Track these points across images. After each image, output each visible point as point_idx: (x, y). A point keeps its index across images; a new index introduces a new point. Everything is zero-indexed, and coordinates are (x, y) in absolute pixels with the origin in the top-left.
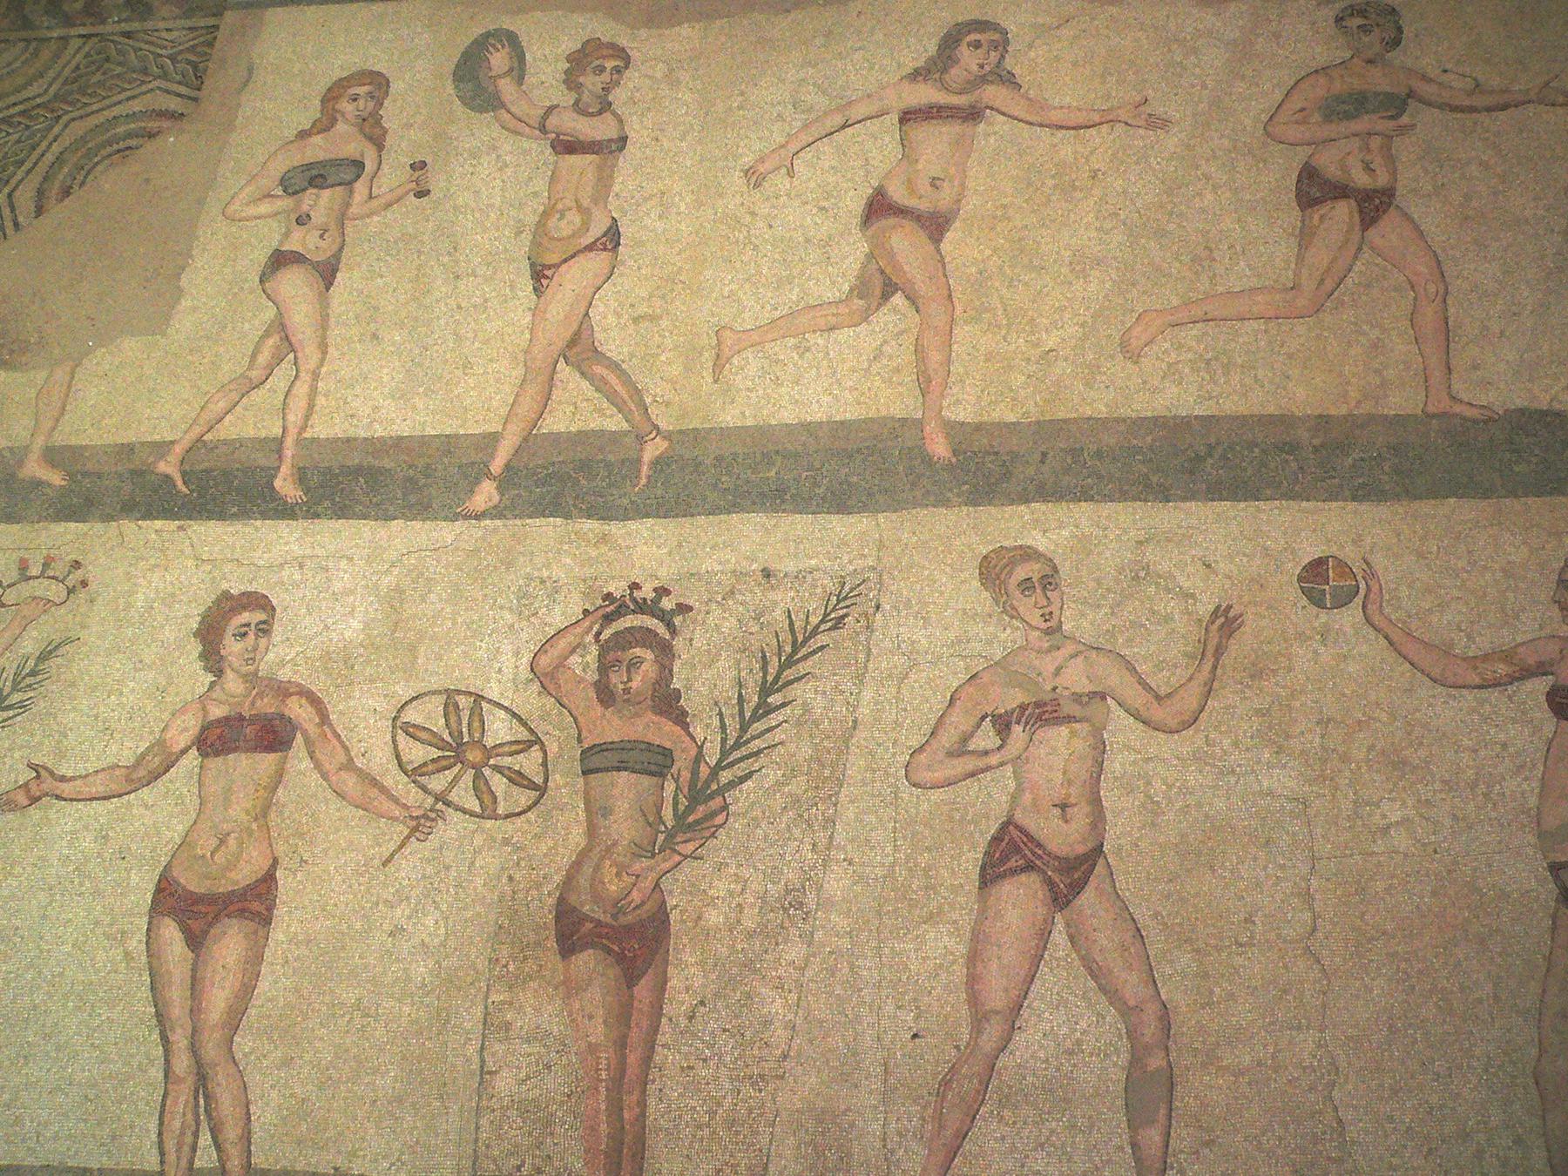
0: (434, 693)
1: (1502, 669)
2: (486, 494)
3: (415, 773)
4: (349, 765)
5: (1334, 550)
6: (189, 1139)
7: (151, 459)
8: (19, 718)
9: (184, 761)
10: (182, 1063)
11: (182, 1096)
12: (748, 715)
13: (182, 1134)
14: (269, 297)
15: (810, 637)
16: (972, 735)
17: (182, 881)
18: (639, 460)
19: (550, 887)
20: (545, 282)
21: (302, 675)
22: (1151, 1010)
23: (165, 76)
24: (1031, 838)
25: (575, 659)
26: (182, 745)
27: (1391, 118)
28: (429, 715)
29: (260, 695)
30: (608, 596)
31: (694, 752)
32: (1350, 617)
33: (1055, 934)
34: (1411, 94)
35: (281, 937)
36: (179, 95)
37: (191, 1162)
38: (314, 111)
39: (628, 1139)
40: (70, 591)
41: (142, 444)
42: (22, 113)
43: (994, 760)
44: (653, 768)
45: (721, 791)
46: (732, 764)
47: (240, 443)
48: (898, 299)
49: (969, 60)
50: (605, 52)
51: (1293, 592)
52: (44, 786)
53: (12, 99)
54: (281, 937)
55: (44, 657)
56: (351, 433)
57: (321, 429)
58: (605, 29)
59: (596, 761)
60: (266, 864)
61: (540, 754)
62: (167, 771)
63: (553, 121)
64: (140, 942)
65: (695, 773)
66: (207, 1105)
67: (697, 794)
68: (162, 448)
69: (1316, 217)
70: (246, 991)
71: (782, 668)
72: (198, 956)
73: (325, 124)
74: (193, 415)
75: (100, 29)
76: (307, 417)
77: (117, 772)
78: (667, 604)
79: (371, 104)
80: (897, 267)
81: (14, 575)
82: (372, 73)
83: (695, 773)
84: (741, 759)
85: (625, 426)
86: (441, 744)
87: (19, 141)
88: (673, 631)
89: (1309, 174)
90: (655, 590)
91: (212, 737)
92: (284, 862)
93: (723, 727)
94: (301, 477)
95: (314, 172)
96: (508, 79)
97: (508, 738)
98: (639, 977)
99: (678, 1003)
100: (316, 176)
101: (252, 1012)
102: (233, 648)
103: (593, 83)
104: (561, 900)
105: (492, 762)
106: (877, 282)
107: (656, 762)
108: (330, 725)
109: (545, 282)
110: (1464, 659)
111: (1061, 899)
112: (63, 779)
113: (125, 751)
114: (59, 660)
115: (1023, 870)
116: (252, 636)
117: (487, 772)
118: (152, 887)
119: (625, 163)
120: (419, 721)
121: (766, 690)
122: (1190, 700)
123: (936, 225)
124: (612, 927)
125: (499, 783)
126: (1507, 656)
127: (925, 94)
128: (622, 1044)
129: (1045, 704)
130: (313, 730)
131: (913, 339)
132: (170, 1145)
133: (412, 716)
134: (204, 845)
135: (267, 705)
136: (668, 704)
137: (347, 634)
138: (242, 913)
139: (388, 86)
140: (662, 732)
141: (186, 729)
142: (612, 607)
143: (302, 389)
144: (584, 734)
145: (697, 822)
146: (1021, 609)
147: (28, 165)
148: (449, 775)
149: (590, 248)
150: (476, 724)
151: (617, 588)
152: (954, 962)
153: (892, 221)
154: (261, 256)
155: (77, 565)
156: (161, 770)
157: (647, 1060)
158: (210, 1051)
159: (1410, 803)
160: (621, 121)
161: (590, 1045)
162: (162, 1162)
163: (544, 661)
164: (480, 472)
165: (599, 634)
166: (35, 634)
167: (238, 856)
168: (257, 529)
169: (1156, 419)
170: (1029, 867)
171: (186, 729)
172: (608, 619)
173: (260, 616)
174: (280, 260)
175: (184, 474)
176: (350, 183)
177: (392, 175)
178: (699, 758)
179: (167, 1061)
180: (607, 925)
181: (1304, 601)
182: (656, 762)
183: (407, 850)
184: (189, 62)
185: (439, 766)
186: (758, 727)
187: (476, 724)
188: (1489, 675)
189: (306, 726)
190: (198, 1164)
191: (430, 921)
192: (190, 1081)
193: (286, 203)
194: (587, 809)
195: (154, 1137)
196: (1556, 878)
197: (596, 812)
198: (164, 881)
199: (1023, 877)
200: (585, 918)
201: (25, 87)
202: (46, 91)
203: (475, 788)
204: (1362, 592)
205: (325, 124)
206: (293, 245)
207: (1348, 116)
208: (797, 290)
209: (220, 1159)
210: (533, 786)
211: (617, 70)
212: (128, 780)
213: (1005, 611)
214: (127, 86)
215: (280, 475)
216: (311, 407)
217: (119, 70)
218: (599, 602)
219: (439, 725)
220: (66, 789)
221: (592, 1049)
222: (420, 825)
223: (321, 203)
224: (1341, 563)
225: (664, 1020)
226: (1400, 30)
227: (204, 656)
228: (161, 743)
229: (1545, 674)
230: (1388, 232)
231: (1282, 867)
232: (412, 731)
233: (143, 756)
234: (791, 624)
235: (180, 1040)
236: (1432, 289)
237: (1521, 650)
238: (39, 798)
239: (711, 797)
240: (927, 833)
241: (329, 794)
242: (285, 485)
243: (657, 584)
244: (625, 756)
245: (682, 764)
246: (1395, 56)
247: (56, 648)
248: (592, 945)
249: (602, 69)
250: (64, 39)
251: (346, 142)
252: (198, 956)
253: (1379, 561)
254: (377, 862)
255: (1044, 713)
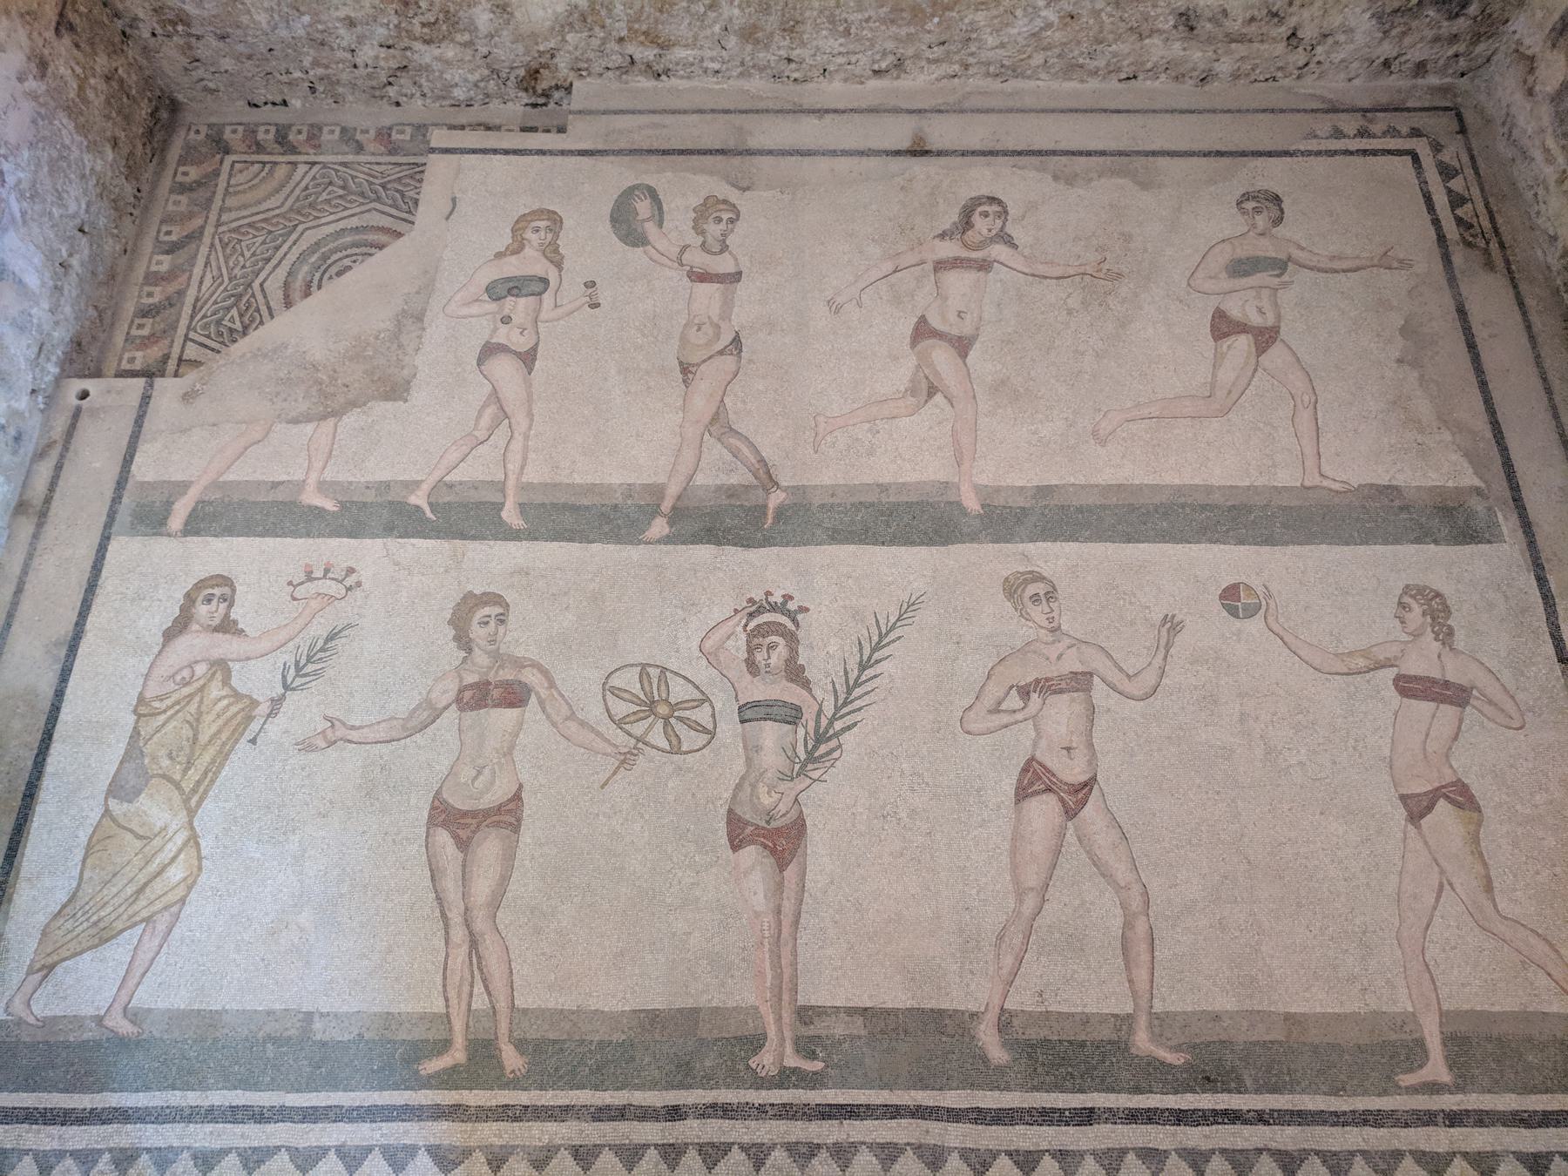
0: (632, 665)
1: (1362, 663)
2: (659, 527)
3: (620, 723)
4: (572, 716)
5: (1243, 579)
6: (466, 989)
7: (404, 493)
8: (314, 683)
9: (446, 714)
10: (458, 934)
11: (460, 954)
12: (851, 683)
13: (460, 986)
14: (485, 376)
15: (890, 631)
16: (1004, 699)
17: (450, 801)
18: (765, 506)
19: (721, 802)
20: (690, 376)
21: (533, 653)
22: (1136, 889)
23: (378, 199)
24: (1049, 771)
25: (730, 643)
26: (444, 703)
27: (1278, 276)
28: (629, 680)
29: (502, 667)
30: (751, 601)
31: (816, 708)
32: (1255, 626)
33: (1068, 835)
34: (1289, 258)
35: (529, 841)
36: (392, 216)
37: (469, 1005)
38: (507, 239)
39: (786, 977)
40: (349, 589)
41: (396, 482)
42: (265, 220)
43: (1019, 716)
44: (790, 719)
45: (837, 735)
46: (842, 717)
47: (475, 486)
48: (938, 398)
49: (981, 225)
50: (722, 207)
51: (1217, 605)
52: (339, 734)
53: (255, 210)
54: (529, 841)
55: (330, 638)
56: (558, 479)
57: (531, 476)
58: (724, 190)
59: (748, 714)
60: (514, 788)
61: (709, 709)
62: (434, 721)
63: (687, 257)
64: (420, 846)
65: (818, 721)
66: (479, 963)
67: (820, 738)
68: (412, 486)
69: (1225, 347)
70: (504, 880)
71: (873, 651)
72: (466, 855)
73: (517, 248)
74: (435, 462)
75: (321, 158)
76: (522, 468)
77: (395, 722)
78: (792, 606)
79: (550, 236)
80: (937, 373)
81: (304, 579)
82: (549, 211)
83: (818, 721)
84: (848, 714)
85: (755, 482)
86: (641, 703)
87: (264, 243)
88: (797, 626)
89: (1220, 316)
90: (784, 596)
91: (468, 695)
92: (526, 787)
93: (835, 691)
94: (523, 508)
95: (511, 284)
96: (651, 223)
97: (687, 698)
98: (788, 865)
99: (815, 881)
100: (514, 287)
101: (509, 895)
102: (477, 632)
103: (714, 229)
104: (730, 811)
105: (676, 714)
106: (924, 385)
107: (793, 716)
108: (557, 689)
109: (690, 376)
110: (1336, 655)
111: (1070, 813)
112: (353, 728)
113: (402, 705)
114: (343, 640)
115: (1044, 791)
116: (492, 623)
117: (673, 721)
118: (427, 807)
119: (742, 290)
120: (622, 686)
121: (863, 667)
122: (1150, 678)
123: (962, 346)
124: (768, 830)
125: (681, 729)
126: (1365, 653)
127: (949, 249)
128: (778, 911)
129: (1052, 679)
130: (544, 693)
131: (949, 427)
132: (452, 994)
133: (616, 681)
134: (466, 773)
135: (507, 674)
136: (795, 673)
137: (565, 624)
138: (497, 824)
139: (561, 222)
140: (791, 693)
141: (445, 692)
142: (754, 608)
143: (517, 445)
144: (740, 696)
145: (821, 756)
146: (1033, 614)
147: (274, 262)
148: (646, 723)
149: (721, 353)
150: (663, 687)
151: (758, 595)
152: (1001, 854)
153: (931, 341)
154: (477, 344)
155: (351, 571)
156: (429, 720)
157: (796, 922)
158: (480, 925)
159: (1303, 751)
160: (736, 260)
161: (756, 912)
162: (447, 1006)
163: (708, 644)
164: (655, 511)
165: (746, 625)
166: (322, 621)
167: (492, 783)
168: (491, 547)
169: (1120, 486)
170: (1049, 790)
171: (445, 692)
172: (751, 615)
173: (499, 610)
174: (490, 350)
175: (430, 504)
176: (540, 294)
177: (572, 291)
178: (820, 712)
179: (447, 933)
180: (763, 828)
181: (1225, 614)
182: (793, 716)
183: (618, 777)
184: (397, 191)
185: (637, 718)
186: (857, 692)
187: (663, 687)
188: (1353, 666)
189: (538, 689)
190: (474, 1006)
191: (637, 826)
192: (465, 948)
193: (492, 307)
194: (745, 747)
195: (440, 988)
196: (1405, 805)
197: (752, 750)
198: (437, 802)
199: (1044, 796)
200: (747, 823)
201: (264, 200)
202: (283, 204)
203: (665, 733)
204: (1264, 608)
205: (517, 248)
206: (500, 338)
207: (1246, 274)
208: (868, 389)
209: (491, 1002)
210: (705, 731)
211: (731, 221)
212: (404, 728)
213: (1022, 615)
214: (348, 205)
215: (506, 507)
216: (525, 459)
217: (341, 192)
218: (745, 604)
219: (636, 688)
220: (354, 735)
221: (757, 914)
222: (626, 760)
223: (520, 307)
224: (1248, 587)
225: (806, 895)
226: (1282, 211)
227: (457, 638)
228: (428, 703)
229: (1392, 666)
230: (1276, 356)
231: (1218, 793)
232: (617, 692)
233: (415, 710)
234: (877, 621)
235: (455, 917)
236: (1306, 398)
237: (1375, 649)
238: (335, 742)
239: (830, 739)
240: (977, 765)
241: (559, 738)
242: (510, 515)
243: (783, 592)
244: (769, 710)
245: (809, 716)
246: (1280, 231)
247: (340, 631)
248: (752, 842)
249: (720, 220)
250: (294, 164)
251: (531, 263)
252: (466, 855)
253: (1274, 587)
254: (596, 786)
255: (1046, 687)
